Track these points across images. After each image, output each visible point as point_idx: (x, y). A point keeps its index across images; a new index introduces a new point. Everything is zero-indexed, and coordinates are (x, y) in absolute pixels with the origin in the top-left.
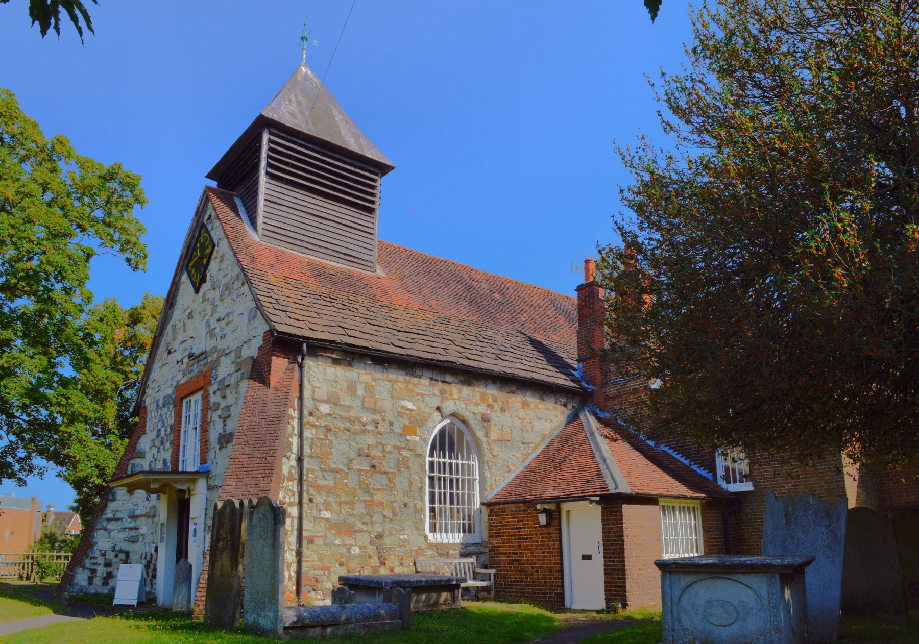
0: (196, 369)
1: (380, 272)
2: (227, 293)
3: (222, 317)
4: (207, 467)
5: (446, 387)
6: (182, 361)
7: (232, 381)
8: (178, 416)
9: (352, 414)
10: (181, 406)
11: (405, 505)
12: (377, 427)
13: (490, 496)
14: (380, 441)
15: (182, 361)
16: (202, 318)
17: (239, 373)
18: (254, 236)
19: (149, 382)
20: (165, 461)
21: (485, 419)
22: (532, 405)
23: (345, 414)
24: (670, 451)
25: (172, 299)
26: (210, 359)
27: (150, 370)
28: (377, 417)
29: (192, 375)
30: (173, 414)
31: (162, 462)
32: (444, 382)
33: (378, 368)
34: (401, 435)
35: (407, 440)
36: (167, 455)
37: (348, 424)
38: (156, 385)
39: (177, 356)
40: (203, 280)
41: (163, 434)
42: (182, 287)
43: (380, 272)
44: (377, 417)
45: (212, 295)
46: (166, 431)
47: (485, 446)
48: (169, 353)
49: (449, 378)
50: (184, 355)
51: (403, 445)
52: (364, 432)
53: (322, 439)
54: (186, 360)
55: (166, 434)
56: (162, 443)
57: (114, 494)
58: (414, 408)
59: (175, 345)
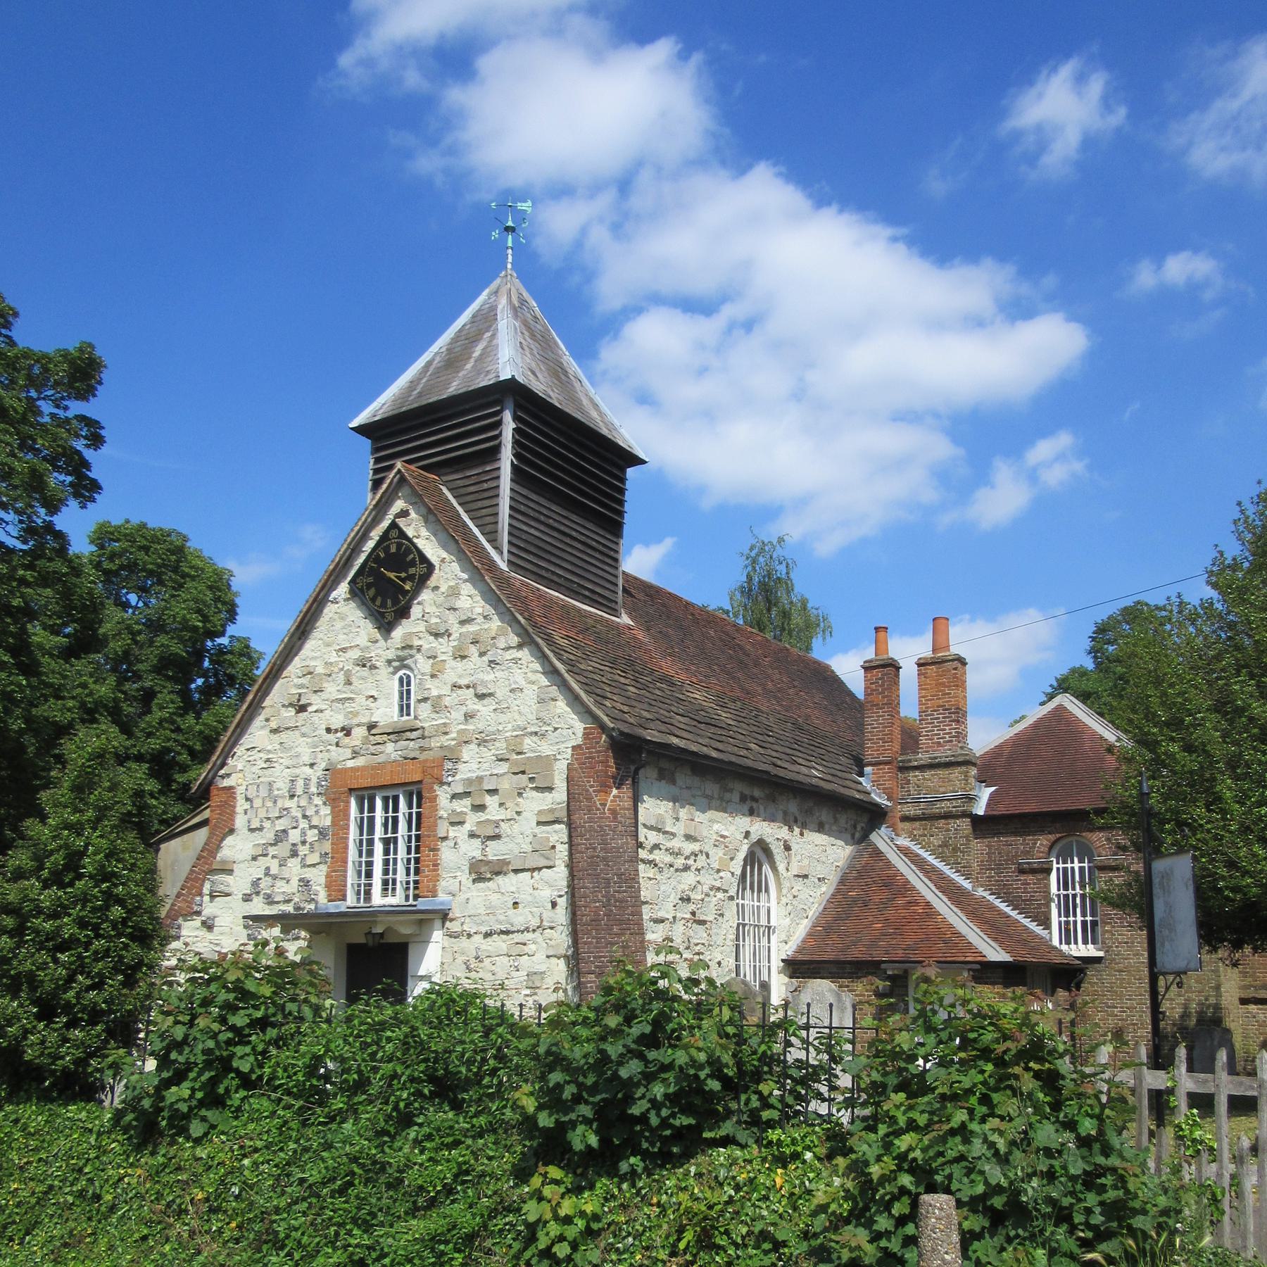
0: (391, 750)
1: (625, 619)
2: (473, 651)
3: (463, 682)
4: (442, 903)
5: (755, 805)
6: (347, 731)
7: (505, 785)
8: (340, 817)
9: (676, 843)
10: (348, 802)
11: (719, 963)
12: (695, 861)
13: (789, 950)
14: (698, 879)
15: (347, 731)
16: (391, 669)
17: (525, 777)
18: (504, 566)
19: (239, 750)
20: (305, 883)
21: (787, 848)
22: (827, 827)
23: (669, 845)
24: (991, 898)
25: (307, 624)
26: (434, 743)
27: (242, 730)
28: (695, 847)
29: (381, 759)
30: (326, 810)
31: (295, 882)
32: (754, 799)
33: (696, 781)
34: (718, 871)
35: (721, 878)
36: (318, 877)
37: (668, 859)
38: (255, 755)
39: (338, 721)
40: (404, 613)
41: (294, 836)
42: (329, 610)
43: (625, 619)
44: (695, 847)
45: (428, 643)
46: (304, 833)
47: (786, 884)
48: (302, 709)
49: (757, 793)
50: (355, 721)
51: (718, 884)
52: (686, 868)
53: (650, 879)
54: (359, 733)
55: (304, 843)
56: (294, 854)
57: (179, 927)
58: (726, 833)
59: (316, 702)
